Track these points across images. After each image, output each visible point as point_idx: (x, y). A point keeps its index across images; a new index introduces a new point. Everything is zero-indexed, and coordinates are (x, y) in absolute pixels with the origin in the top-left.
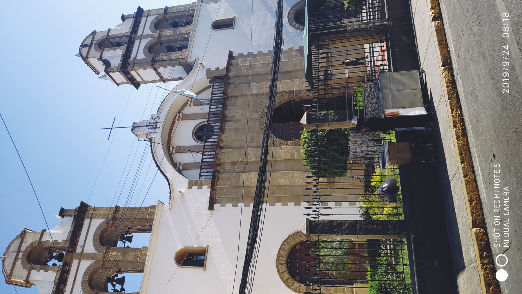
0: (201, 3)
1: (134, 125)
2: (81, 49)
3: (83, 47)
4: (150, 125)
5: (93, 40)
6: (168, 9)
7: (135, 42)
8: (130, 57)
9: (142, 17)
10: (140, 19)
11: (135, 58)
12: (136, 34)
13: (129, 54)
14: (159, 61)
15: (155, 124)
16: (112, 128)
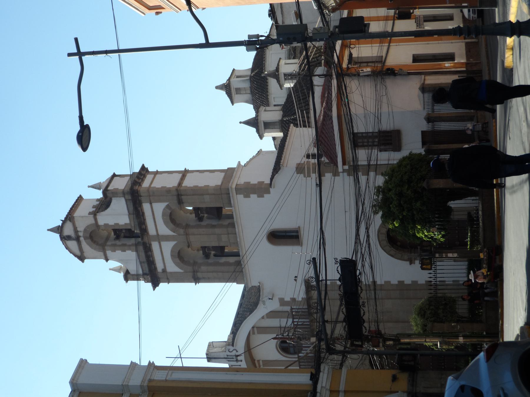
0: (236, 194)
1: (209, 357)
2: (65, 242)
3: (67, 240)
4: (228, 357)
5: (76, 231)
6: (181, 195)
7: (151, 244)
8: (156, 268)
9: (142, 204)
10: (141, 210)
11: (164, 271)
12: (148, 233)
13: (153, 266)
14: (204, 278)
15: (235, 357)
16: (181, 358)
